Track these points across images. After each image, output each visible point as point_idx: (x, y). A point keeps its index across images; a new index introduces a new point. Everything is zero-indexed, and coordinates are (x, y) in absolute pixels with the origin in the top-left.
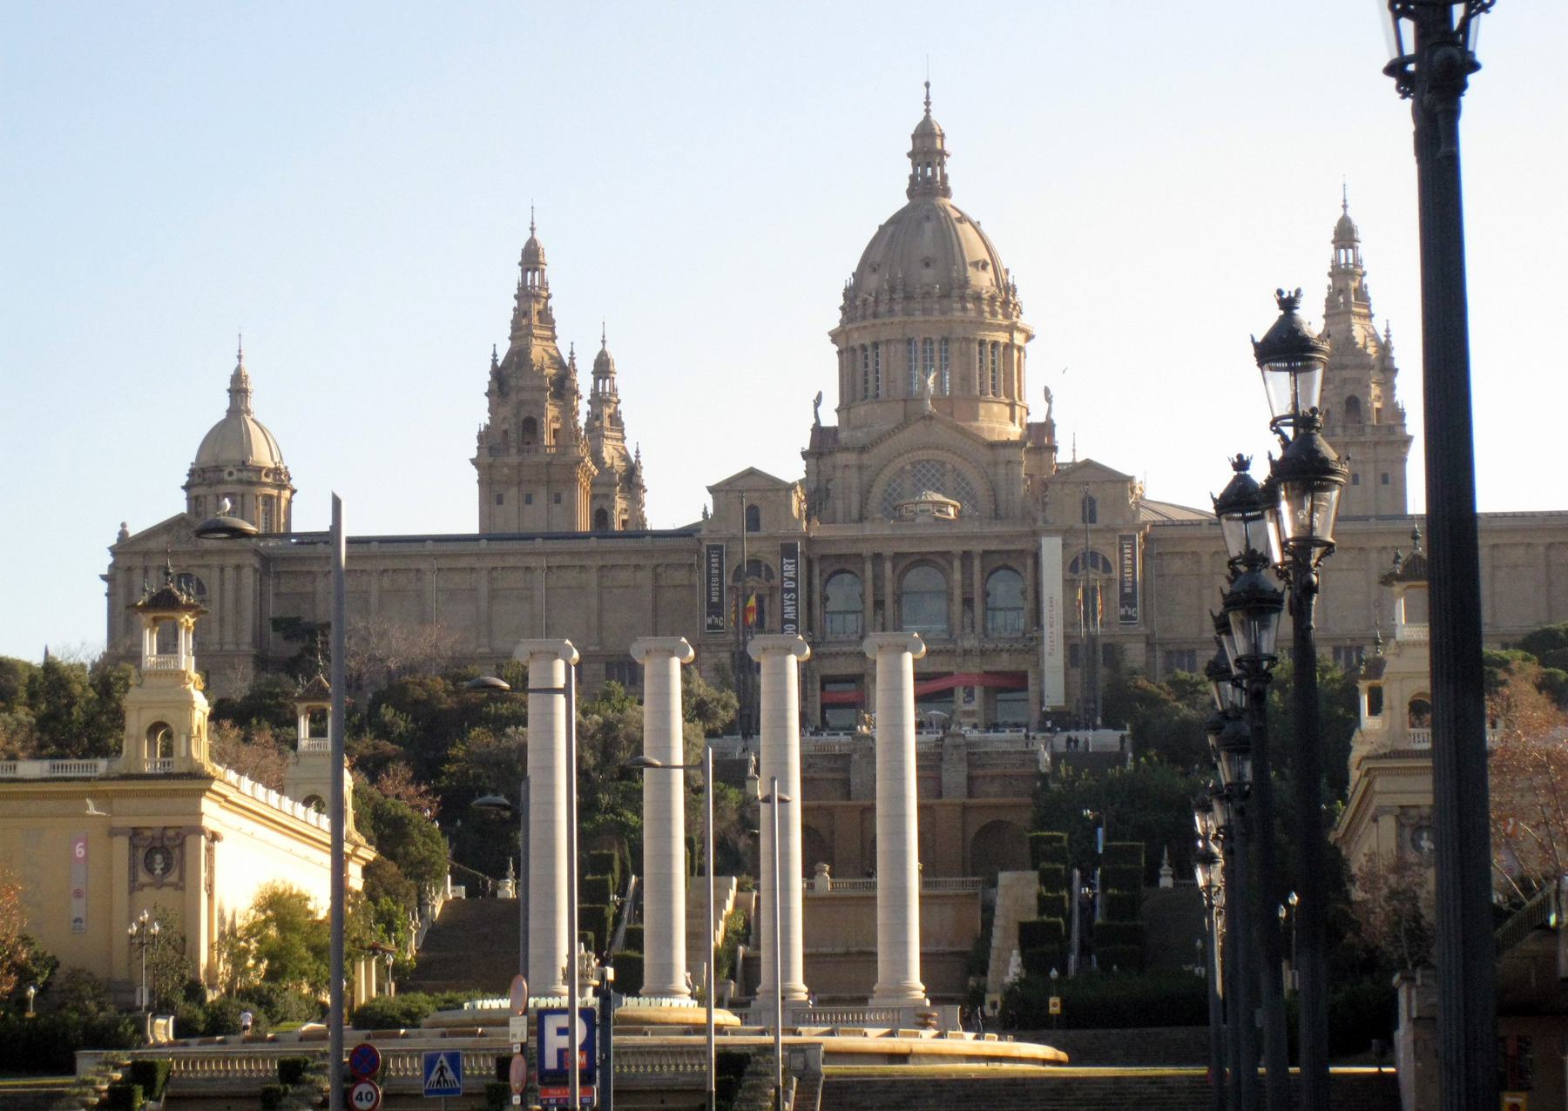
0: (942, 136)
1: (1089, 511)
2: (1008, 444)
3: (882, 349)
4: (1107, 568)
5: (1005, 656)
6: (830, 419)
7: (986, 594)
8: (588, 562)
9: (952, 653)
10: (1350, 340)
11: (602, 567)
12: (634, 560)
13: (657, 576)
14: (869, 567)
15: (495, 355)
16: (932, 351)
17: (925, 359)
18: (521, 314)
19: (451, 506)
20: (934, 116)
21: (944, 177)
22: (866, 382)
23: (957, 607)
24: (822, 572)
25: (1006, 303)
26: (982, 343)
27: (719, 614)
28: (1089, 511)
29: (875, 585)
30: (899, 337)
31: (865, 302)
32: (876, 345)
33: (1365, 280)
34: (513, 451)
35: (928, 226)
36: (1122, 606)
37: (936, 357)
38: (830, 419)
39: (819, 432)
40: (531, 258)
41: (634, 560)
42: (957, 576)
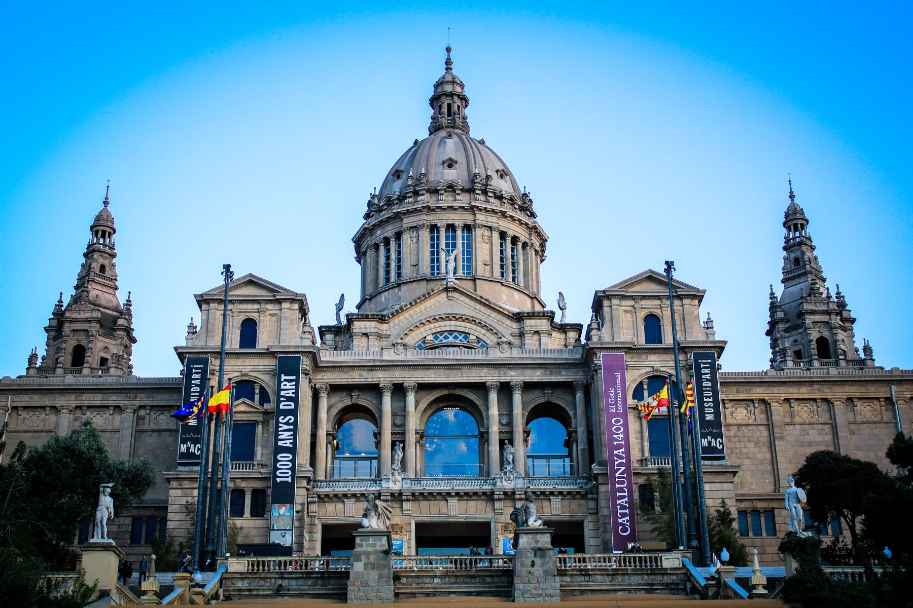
0: (462, 86)
3: (406, 237)
5: (556, 501)
8: (60, 401)
9: (489, 497)
10: (813, 292)
11: (77, 407)
12: (113, 400)
13: (140, 419)
14: (387, 399)
15: (61, 301)
16: (454, 238)
17: (447, 245)
18: (87, 268)
20: (454, 72)
21: (465, 118)
22: (388, 272)
23: (494, 448)
24: (329, 409)
27: (195, 442)
29: (394, 425)
30: (421, 223)
31: (389, 202)
32: (398, 236)
33: (815, 253)
34: (59, 371)
36: (704, 436)
37: (459, 242)
40: (102, 228)
42: (494, 411)
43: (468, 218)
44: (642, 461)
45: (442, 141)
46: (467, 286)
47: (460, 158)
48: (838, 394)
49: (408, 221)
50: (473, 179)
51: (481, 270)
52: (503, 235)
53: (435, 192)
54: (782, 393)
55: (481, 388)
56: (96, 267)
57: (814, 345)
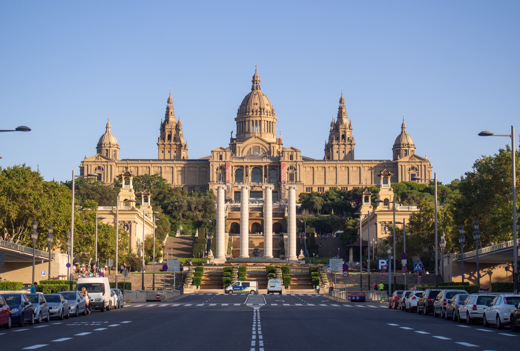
1: (291, 157)
2: (273, 143)
4: (295, 170)
6: (234, 137)
7: (269, 175)
12: (195, 166)
19: (154, 153)
25: (273, 113)
26: (267, 121)
28: (291, 157)
32: (245, 121)
35: (257, 96)
38: (234, 137)
39: (232, 140)
41: (195, 166)
43: (260, 119)
44: (288, 182)
45: (255, 97)
46: (259, 135)
47: (258, 102)
48: (326, 166)
49: (247, 119)
50: (260, 108)
51: (263, 131)
52: (267, 121)
53: (253, 112)
54: (317, 165)
55: (261, 166)
56: (170, 113)
57: (341, 137)
